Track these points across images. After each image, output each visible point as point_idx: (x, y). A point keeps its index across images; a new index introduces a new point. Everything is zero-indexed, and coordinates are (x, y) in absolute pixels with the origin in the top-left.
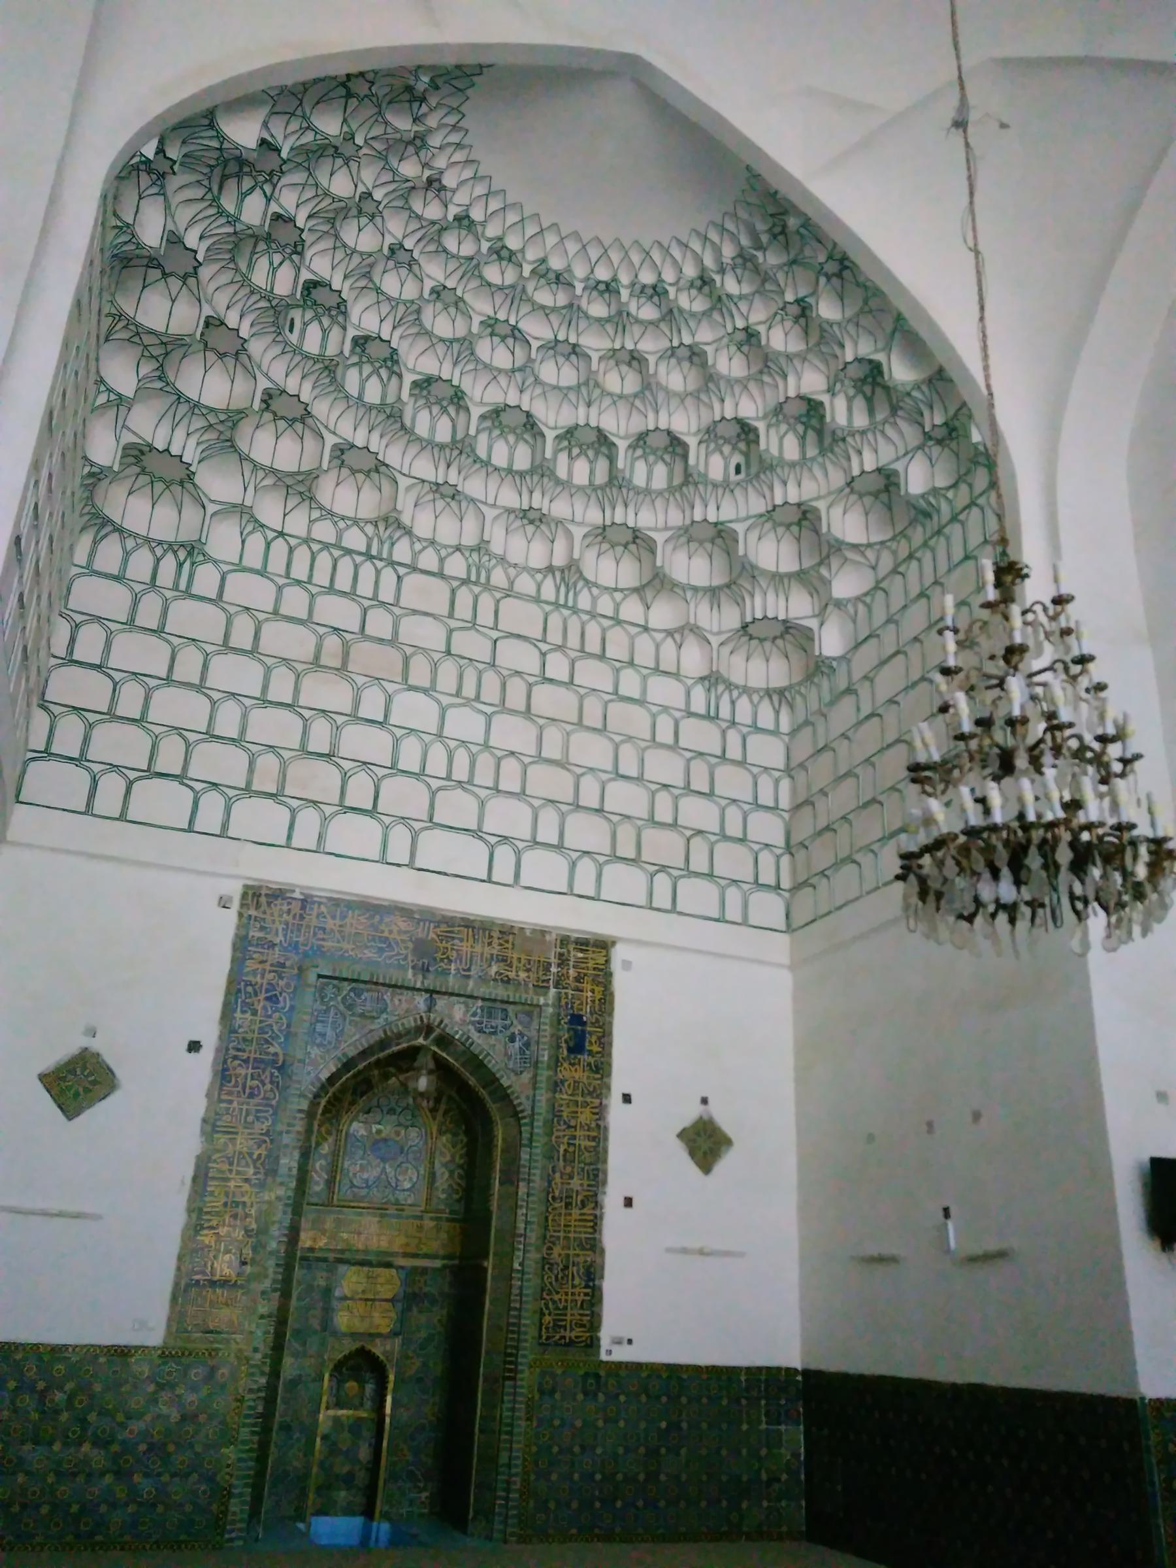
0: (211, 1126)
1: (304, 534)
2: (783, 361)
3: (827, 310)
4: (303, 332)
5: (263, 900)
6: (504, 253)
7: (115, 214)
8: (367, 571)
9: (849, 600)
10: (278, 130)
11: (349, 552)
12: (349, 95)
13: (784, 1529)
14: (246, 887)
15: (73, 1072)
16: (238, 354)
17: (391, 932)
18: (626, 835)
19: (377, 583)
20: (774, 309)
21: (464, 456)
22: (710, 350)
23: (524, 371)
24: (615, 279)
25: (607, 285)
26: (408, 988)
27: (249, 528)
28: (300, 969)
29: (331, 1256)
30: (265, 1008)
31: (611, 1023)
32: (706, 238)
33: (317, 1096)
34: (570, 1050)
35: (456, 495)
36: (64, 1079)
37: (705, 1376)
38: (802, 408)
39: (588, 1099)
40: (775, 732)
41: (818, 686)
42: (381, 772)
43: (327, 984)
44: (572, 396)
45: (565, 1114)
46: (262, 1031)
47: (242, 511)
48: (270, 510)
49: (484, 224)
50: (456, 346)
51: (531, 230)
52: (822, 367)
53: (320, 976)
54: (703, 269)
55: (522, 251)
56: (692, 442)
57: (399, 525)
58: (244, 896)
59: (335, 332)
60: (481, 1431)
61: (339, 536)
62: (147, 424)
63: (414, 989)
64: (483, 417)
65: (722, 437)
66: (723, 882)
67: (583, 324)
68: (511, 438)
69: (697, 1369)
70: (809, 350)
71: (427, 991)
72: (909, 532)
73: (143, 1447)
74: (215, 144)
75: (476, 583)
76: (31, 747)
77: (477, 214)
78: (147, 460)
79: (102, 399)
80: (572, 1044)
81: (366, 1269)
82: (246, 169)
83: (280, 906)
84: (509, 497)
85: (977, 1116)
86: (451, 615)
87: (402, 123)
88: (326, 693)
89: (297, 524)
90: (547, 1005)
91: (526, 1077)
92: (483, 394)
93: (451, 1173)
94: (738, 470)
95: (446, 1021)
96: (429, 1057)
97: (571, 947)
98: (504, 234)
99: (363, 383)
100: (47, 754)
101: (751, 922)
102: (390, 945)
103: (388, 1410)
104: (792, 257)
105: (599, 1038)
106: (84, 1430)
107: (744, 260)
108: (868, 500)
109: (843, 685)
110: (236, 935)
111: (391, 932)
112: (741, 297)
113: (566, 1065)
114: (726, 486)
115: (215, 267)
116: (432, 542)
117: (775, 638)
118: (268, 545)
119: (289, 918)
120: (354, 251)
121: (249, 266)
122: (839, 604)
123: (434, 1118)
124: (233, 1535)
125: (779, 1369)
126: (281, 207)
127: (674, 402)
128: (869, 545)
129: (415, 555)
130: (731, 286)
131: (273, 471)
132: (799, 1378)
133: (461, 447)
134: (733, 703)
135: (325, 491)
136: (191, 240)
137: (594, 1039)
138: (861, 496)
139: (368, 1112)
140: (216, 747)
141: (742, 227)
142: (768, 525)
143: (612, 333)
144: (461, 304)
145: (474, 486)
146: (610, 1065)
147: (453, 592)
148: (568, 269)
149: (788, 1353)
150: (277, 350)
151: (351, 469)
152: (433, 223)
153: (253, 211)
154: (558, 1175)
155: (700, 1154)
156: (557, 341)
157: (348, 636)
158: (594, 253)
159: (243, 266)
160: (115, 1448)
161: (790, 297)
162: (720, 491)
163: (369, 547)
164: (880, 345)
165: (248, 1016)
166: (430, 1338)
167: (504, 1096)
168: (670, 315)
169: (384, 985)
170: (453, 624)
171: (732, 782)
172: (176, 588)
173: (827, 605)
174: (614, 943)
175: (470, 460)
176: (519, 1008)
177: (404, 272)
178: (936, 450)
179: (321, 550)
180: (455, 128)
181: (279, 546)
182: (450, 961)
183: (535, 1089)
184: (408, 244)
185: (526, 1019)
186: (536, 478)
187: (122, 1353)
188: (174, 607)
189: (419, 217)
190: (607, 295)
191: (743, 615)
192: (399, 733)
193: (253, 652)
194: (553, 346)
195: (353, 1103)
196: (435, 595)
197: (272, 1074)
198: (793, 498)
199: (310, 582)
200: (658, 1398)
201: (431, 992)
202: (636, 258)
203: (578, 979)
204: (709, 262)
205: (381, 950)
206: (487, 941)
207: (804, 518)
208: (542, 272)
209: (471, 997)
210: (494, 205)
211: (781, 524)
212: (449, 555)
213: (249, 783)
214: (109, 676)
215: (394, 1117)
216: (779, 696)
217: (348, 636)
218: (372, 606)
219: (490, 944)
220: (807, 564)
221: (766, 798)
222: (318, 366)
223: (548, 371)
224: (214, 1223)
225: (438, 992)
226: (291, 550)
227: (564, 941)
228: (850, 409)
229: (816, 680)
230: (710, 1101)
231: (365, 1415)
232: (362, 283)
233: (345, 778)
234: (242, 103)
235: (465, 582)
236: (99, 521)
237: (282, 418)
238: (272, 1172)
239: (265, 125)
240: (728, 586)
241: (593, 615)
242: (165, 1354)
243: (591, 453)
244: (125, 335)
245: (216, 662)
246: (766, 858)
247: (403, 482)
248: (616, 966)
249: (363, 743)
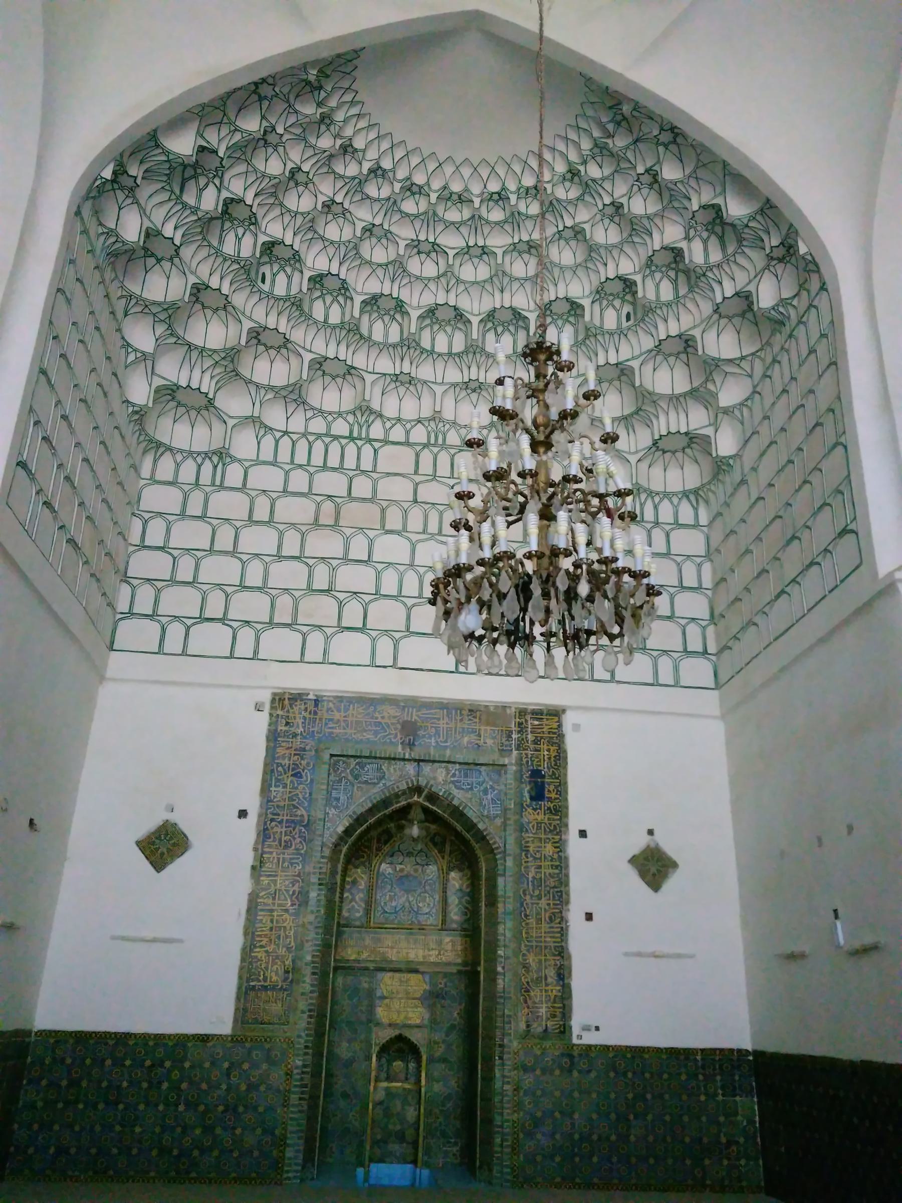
1: (302, 430)
2: (645, 222)
3: (670, 172)
4: (273, 281)
5: (286, 702)
6: (415, 189)
7: (101, 224)
8: (351, 449)
9: (734, 407)
10: (212, 137)
11: (336, 438)
12: (261, 99)
13: (744, 1184)
14: (274, 694)
15: (159, 838)
16: (226, 307)
17: (383, 718)
19: (358, 458)
20: (631, 182)
21: (412, 350)
22: (587, 227)
23: (447, 277)
24: (504, 188)
25: (499, 194)
26: (399, 759)
27: (262, 432)
28: (316, 751)
29: (371, 966)
30: (292, 782)
31: (566, 775)
32: (567, 139)
33: (336, 845)
34: (532, 798)
35: (411, 381)
36: (153, 843)
37: (664, 1057)
38: (669, 256)
39: (550, 836)
40: (696, 526)
41: (723, 483)
42: (367, 598)
43: (338, 761)
44: (488, 287)
45: (531, 849)
46: (291, 799)
47: (253, 420)
48: (275, 416)
49: (393, 170)
50: (390, 267)
51: (432, 166)
52: (679, 219)
53: (332, 755)
54: (569, 163)
55: (428, 183)
56: (586, 303)
57: (372, 412)
58: (273, 701)
59: (297, 275)
60: (481, 1100)
61: (329, 427)
62: (171, 369)
63: (404, 760)
64: (421, 317)
65: (611, 294)
66: (655, 653)
67: (486, 230)
68: (449, 329)
69: (658, 1050)
70: (664, 209)
71: (415, 760)
72: (771, 341)
73: (221, 1108)
74: (164, 158)
75: (434, 445)
76: (119, 610)
77: (387, 164)
78: (180, 396)
79: (132, 357)
80: (533, 794)
81: (397, 975)
82: (199, 171)
83: (299, 706)
84: (454, 375)
85: (850, 829)
86: (416, 472)
87: (309, 109)
88: (325, 544)
89: (297, 423)
90: (511, 764)
91: (499, 821)
92: (418, 299)
93: (460, 899)
94: (628, 318)
95: (432, 782)
96: (419, 810)
97: (528, 717)
98: (410, 175)
99: (327, 309)
100: (131, 614)
101: (682, 684)
102: (383, 727)
103: (423, 1082)
104: (635, 137)
105: (556, 787)
106: (179, 1096)
107: (600, 150)
108: (737, 321)
109: (738, 478)
110: (269, 730)
111: (383, 718)
112: (603, 179)
113: (530, 810)
114: (621, 333)
115: (194, 247)
116: (399, 420)
117: (684, 449)
118: (277, 442)
119: (307, 715)
120: (296, 213)
121: (220, 242)
122: (726, 411)
123: (443, 858)
124: (290, 1175)
125: (731, 1051)
126: (232, 193)
127: (568, 275)
128: (742, 358)
129: (387, 432)
130: (594, 171)
131: (271, 388)
132: (751, 1058)
133: (408, 345)
134: (656, 507)
135: (316, 395)
136: (168, 231)
137: (552, 788)
138: (730, 318)
139: (392, 856)
140: (246, 594)
141: (593, 125)
142: (659, 358)
143: (510, 231)
144: (389, 235)
145: (425, 371)
146: (567, 808)
147: (417, 455)
148: (467, 190)
149: (740, 1037)
150: (256, 298)
151: (331, 376)
152: (354, 178)
153: (210, 201)
154: (528, 897)
155: (649, 877)
156: (468, 247)
157: (339, 500)
158: (484, 172)
159: (215, 243)
160: (202, 1108)
161: (640, 169)
162: (616, 337)
163: (351, 432)
164: (719, 189)
165: (280, 789)
166: (453, 1027)
167: (482, 838)
168: (551, 207)
169: (381, 758)
170: (418, 479)
172: (213, 484)
173: (720, 413)
174: (564, 711)
175: (418, 352)
176: (491, 767)
177: (341, 220)
178: (780, 268)
179: (317, 439)
180: (352, 103)
181: (285, 442)
182: (430, 737)
183: (505, 830)
184: (339, 199)
185: (495, 776)
186: (470, 356)
187: (204, 1039)
188: (213, 498)
189: (342, 177)
190: (501, 203)
191: (653, 434)
192: (380, 567)
193: (270, 522)
195: (379, 849)
196: (402, 459)
197: (300, 831)
198: (674, 330)
199: (308, 465)
200: (625, 1074)
201: (419, 761)
202: (517, 168)
203: (536, 742)
204: (573, 156)
205: (376, 733)
206: (459, 718)
207: (687, 344)
208: (448, 197)
209: (448, 762)
210: (399, 153)
211: (670, 355)
212: (412, 427)
213: (271, 618)
214: (170, 554)
215: (413, 859)
216: (694, 495)
217: (339, 500)
218: (356, 475)
219: (461, 720)
220: (696, 384)
221: (690, 580)
222: (288, 304)
223: (467, 272)
224: (263, 943)
225: (423, 761)
226: (294, 443)
227: (522, 712)
228: (706, 249)
229: (720, 477)
230: (656, 832)
231: (407, 1086)
232: (310, 236)
233: (341, 605)
234: (176, 124)
236: (154, 445)
237: (271, 347)
238: (306, 902)
239: (200, 134)
240: (637, 412)
242: (235, 1039)
243: (512, 328)
244: (139, 309)
245: (245, 534)
246: (693, 631)
247: (369, 378)
248: (567, 728)
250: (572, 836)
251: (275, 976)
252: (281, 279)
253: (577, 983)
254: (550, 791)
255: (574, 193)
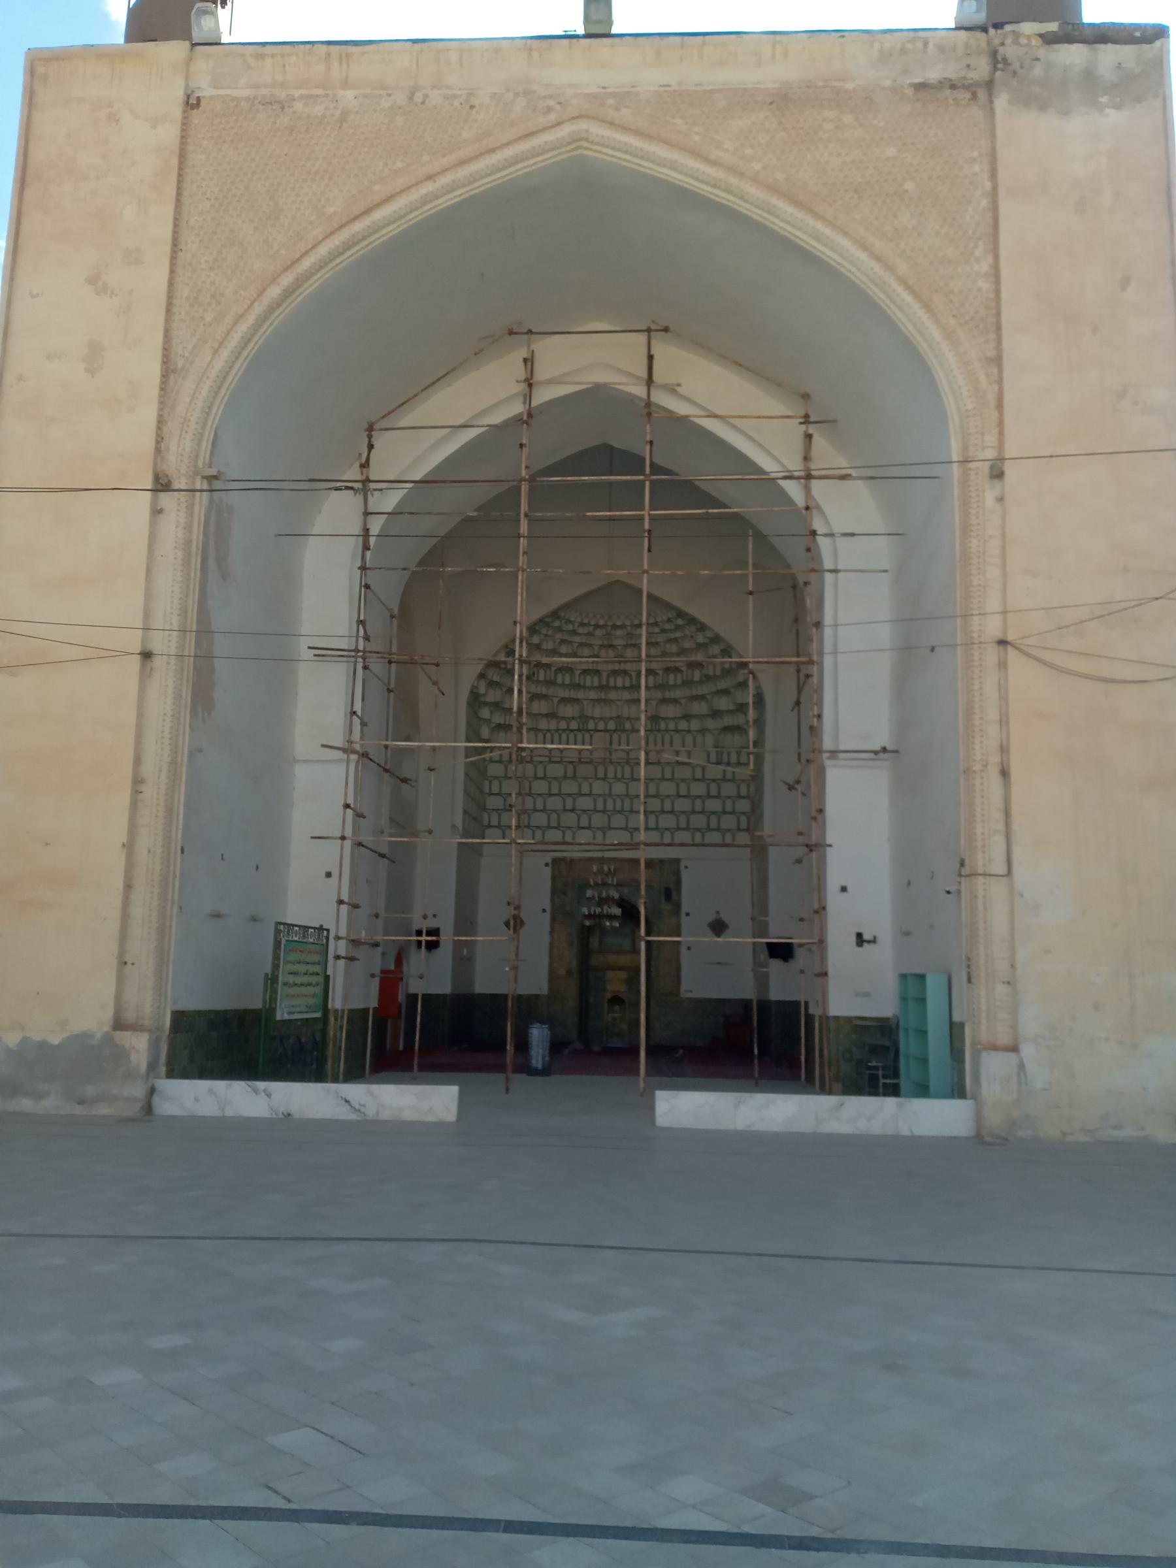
0: (552, 932)
11: (572, 731)
18: (683, 819)
77: (586, 621)
88: (570, 787)
92: (605, 668)
100: (490, 826)
133: (601, 688)
171: (729, 789)
187: (537, 996)
194: (626, 646)
227: (662, 861)
235: (615, 731)
241: (667, 731)
249: (584, 803)
250: (683, 915)
251: (562, 972)
252: (542, 672)
253: (683, 974)
254: (674, 896)
255: (672, 627)
